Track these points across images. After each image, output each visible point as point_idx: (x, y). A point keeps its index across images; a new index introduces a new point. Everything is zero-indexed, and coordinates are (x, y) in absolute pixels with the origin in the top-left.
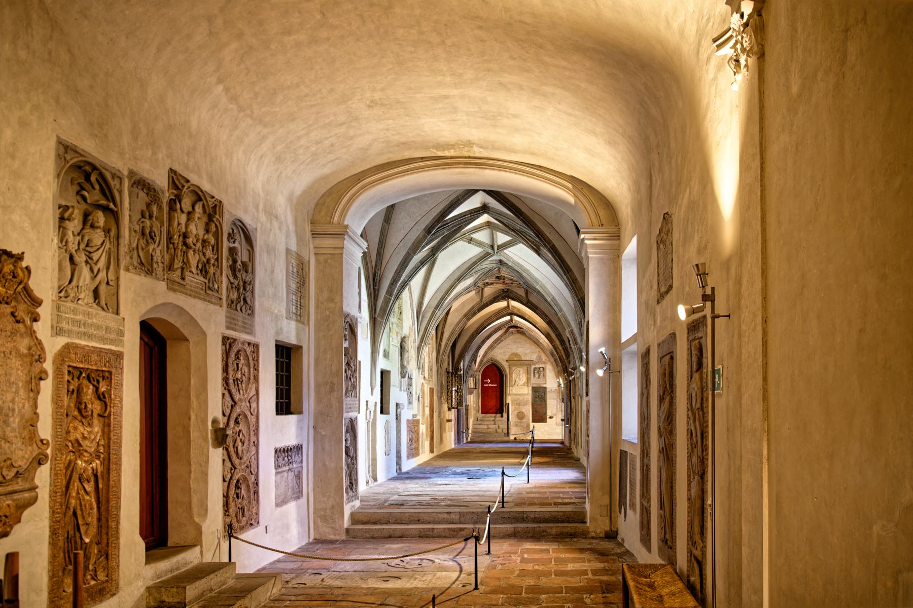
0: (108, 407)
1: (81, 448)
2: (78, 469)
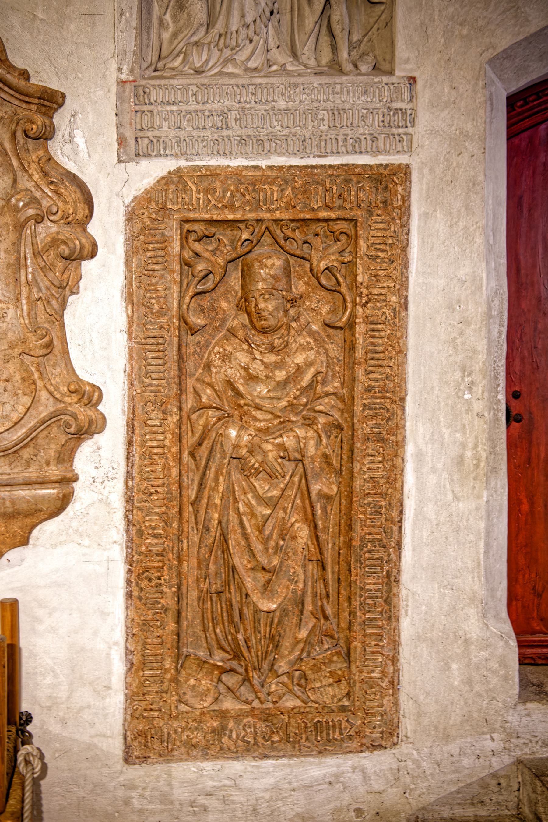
0: (349, 305)
1: (242, 402)
2: (228, 449)
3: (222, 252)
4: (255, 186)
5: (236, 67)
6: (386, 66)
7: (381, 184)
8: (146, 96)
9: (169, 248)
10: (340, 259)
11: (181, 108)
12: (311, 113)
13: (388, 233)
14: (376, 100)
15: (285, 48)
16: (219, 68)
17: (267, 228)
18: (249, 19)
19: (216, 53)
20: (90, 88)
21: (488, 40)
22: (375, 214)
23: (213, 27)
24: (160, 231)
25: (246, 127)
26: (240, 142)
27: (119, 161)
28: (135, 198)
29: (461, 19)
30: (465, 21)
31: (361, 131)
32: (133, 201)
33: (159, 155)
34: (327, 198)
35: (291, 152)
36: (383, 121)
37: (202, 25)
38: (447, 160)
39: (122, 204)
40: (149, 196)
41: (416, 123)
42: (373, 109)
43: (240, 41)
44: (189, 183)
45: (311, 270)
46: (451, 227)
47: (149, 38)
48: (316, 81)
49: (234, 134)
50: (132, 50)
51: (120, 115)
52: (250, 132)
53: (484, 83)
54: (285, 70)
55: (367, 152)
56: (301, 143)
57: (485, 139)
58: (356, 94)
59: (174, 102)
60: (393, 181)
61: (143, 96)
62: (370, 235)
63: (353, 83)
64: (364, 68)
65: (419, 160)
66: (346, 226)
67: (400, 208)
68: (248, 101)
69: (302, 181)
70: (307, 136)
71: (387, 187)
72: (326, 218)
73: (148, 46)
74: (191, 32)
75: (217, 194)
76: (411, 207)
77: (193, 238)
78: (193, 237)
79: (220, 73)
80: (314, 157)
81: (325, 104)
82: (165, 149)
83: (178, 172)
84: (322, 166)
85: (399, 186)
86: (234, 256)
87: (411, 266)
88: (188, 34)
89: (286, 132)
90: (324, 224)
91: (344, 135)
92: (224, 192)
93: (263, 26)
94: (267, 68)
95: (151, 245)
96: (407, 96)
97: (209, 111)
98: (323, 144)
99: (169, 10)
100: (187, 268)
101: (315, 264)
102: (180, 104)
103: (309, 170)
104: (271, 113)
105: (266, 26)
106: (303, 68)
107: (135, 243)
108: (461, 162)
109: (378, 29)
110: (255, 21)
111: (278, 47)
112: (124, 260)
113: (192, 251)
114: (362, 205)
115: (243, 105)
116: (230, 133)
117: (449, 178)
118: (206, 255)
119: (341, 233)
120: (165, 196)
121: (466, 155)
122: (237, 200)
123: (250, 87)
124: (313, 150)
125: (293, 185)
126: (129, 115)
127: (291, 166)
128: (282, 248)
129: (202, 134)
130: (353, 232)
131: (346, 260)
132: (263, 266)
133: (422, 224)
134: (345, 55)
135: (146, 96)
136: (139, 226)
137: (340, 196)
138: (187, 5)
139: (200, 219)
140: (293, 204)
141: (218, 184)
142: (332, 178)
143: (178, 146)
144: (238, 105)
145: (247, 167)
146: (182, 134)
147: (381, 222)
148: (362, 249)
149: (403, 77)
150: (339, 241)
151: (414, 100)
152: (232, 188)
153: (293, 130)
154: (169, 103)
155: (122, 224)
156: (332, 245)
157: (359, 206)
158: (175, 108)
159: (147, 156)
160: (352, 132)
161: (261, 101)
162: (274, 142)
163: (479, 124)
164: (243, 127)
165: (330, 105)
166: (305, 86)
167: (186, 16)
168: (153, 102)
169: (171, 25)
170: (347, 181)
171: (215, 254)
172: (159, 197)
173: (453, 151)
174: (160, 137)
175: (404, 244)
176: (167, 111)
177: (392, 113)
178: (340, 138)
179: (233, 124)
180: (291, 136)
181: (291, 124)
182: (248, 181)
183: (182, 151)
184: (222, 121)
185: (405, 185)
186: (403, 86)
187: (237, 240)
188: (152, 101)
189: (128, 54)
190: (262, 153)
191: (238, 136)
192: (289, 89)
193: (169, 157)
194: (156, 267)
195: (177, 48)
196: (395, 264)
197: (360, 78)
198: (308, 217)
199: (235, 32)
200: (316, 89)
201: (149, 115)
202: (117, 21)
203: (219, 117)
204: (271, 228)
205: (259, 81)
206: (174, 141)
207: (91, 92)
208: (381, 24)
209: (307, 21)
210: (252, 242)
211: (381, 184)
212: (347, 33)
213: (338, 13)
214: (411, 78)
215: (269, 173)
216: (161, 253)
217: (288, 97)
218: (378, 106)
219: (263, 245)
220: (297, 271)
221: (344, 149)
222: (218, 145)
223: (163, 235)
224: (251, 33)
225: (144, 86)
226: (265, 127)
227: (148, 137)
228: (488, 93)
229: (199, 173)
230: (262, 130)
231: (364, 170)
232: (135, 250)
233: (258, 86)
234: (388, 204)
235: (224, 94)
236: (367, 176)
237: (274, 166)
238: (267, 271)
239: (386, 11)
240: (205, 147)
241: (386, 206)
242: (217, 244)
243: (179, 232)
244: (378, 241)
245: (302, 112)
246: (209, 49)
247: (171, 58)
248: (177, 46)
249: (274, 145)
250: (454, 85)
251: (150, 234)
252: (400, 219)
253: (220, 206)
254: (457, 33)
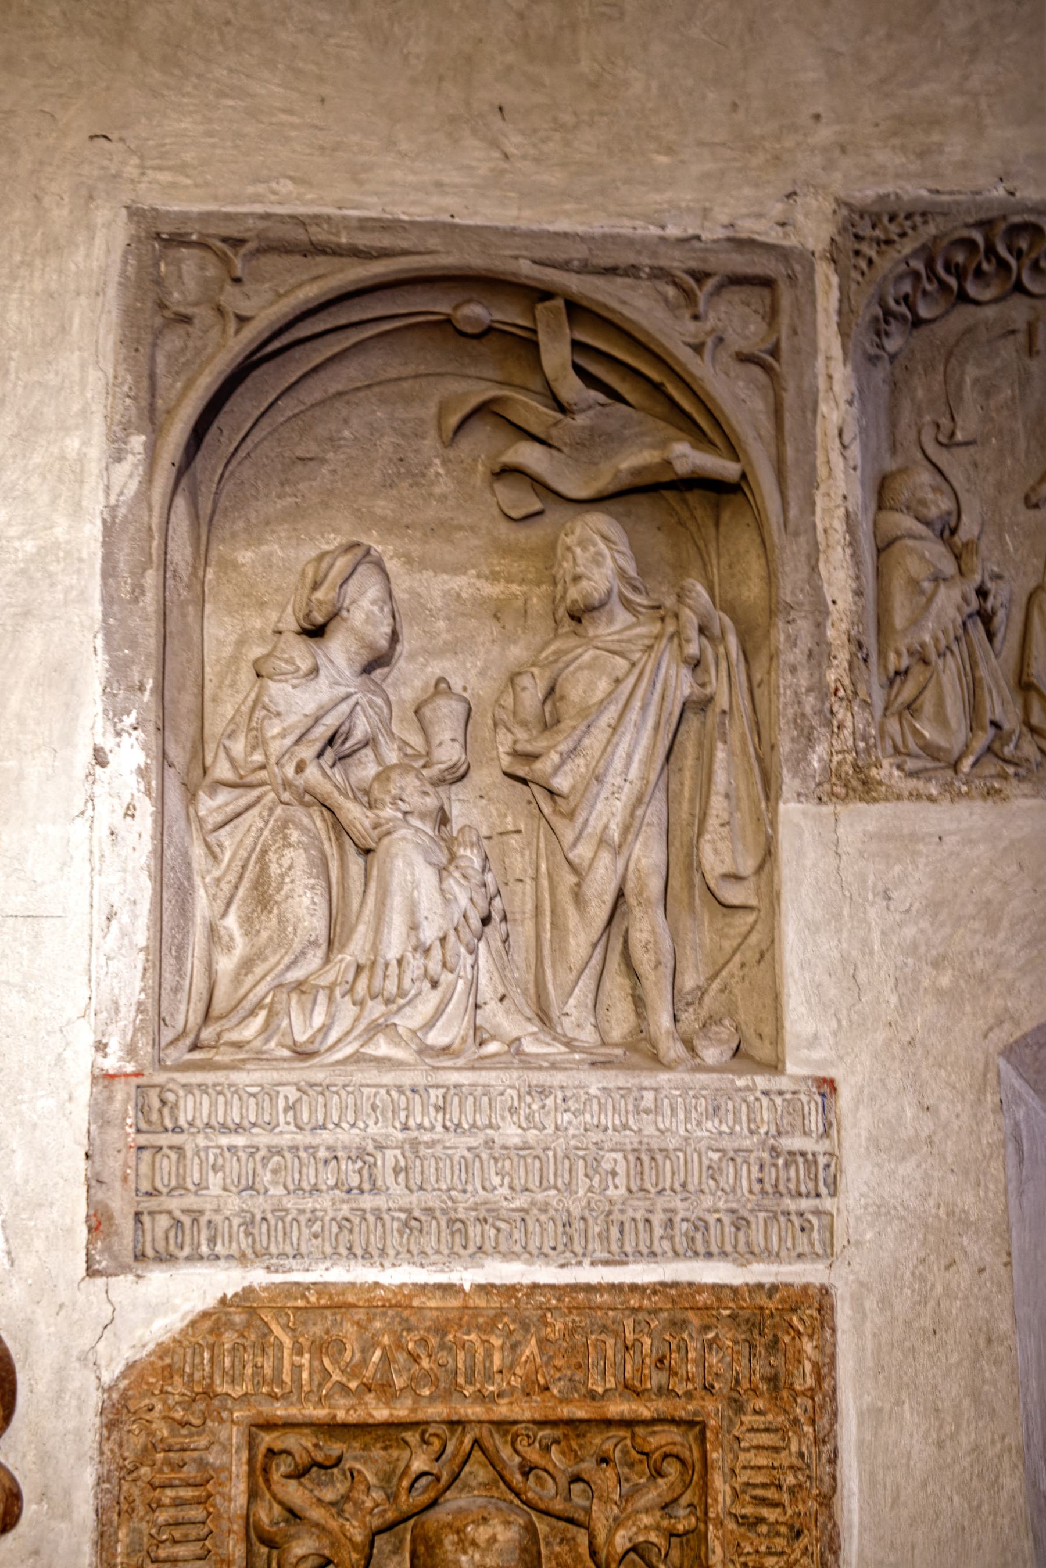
3: (358, 1505)
4: (445, 1334)
5: (397, 1045)
6: (763, 1051)
7: (761, 1334)
8: (166, 1111)
9: (218, 1500)
10: (665, 1523)
11: (256, 1140)
12: (583, 1158)
13: (784, 1459)
14: (742, 1128)
15: (520, 999)
16: (355, 1046)
17: (476, 1442)
18: (429, 934)
19: (347, 1011)
20: (22, 1091)
21: (1000, 1002)
22: (749, 1408)
23: (343, 946)
24: (196, 1454)
25: (421, 1188)
26: (406, 1224)
27: (91, 1272)
28: (130, 1367)
29: (934, 952)
30: (944, 958)
31: (708, 1202)
32: (123, 1375)
33: (196, 1257)
34: (628, 1367)
35: (535, 1252)
36: (761, 1181)
37: (314, 944)
38: (922, 1279)
39: (94, 1383)
40: (168, 1361)
41: (841, 1187)
42: (736, 1151)
43: (407, 983)
44: (274, 1326)
45: (593, 1553)
46: (940, 1445)
47: (180, 971)
48: (595, 1082)
49: (391, 1205)
50: (134, 1000)
51: (97, 1158)
52: (432, 1200)
53: (997, 1099)
54: (519, 1052)
55: (724, 1254)
56: (560, 1229)
57: (1009, 1230)
58: (694, 1115)
59: (239, 1126)
60: (791, 1326)
61: (160, 1111)
62: (739, 1464)
63: (685, 1090)
64: (711, 1054)
65: (851, 1277)
66: (678, 1439)
67: (810, 1394)
68: (427, 1124)
69: (565, 1324)
70: (576, 1213)
71: (776, 1340)
72: (627, 1416)
73: (176, 990)
74: (287, 960)
75: (347, 1355)
76: (839, 1392)
77: (283, 1469)
78: (282, 1467)
79: (357, 1059)
80: (593, 1264)
81: (617, 1137)
82: (212, 1241)
83: (247, 1299)
84: (612, 1286)
85: (805, 1339)
86: (390, 1516)
87: (845, 1546)
88: (278, 963)
89: (521, 1201)
90: (622, 1433)
91: (665, 1211)
92: (366, 1351)
93: (463, 950)
94: (474, 1049)
95: (170, 1493)
96: (815, 1122)
97: (328, 1148)
98: (614, 1232)
99: (233, 908)
100: (264, 1550)
101: (601, 1538)
102: (255, 1130)
103: (581, 1296)
104: (485, 1156)
105: (473, 951)
106: (563, 1049)
107: (125, 1486)
108: (954, 1285)
109: (743, 965)
110: (443, 940)
111: (502, 999)
112: (95, 1536)
113: (281, 1503)
114: (717, 1386)
115: (415, 1134)
116: (381, 1201)
117: (926, 1322)
118: (316, 1514)
119: (666, 1456)
120: (212, 1360)
121: (965, 1272)
122: (399, 1372)
123: (433, 1092)
124: (590, 1247)
125: (543, 1334)
126: (121, 1156)
127: (535, 1286)
128: (518, 1495)
129: (309, 1204)
130: (696, 1455)
131: (680, 1528)
132: (465, 1543)
133: (868, 1437)
134: (665, 1021)
135: (166, 1111)
136: (138, 1441)
137: (661, 1360)
138: (278, 898)
139: (300, 1419)
140: (542, 1381)
141: (349, 1329)
142: (640, 1316)
143: (248, 1234)
144: (400, 1136)
145: (424, 1286)
146: (259, 1205)
147: (767, 1430)
148: (720, 1498)
149: (805, 1078)
150: (661, 1475)
151: (834, 1132)
152: (386, 1340)
153: (540, 1197)
154: (225, 1128)
155: (91, 1439)
156: (644, 1486)
157: (709, 1389)
158: (240, 1140)
159: (166, 1258)
160: (686, 1204)
161: (458, 1125)
162: (494, 1226)
163: (991, 1195)
164: (414, 1187)
165: (629, 1139)
166: (569, 1094)
167: (274, 921)
168: (185, 1126)
169: (239, 940)
170: (678, 1325)
171: (341, 1513)
172: (193, 1365)
173: (932, 1258)
174: (201, 1212)
175: (826, 1489)
176: (220, 1147)
177: (781, 1162)
178: (657, 1219)
179: (390, 1180)
180: (535, 1211)
181: (534, 1183)
182: (428, 1324)
183: (258, 1247)
184: (360, 1171)
185: (822, 1337)
186: (804, 1099)
187: (399, 1472)
188: (182, 1122)
189: (123, 1010)
190: (462, 1252)
191: (401, 1210)
192: (528, 1099)
193: (222, 1263)
194: (182, 1551)
195: (251, 996)
196: (804, 1541)
197: (702, 1077)
198: (581, 1414)
199: (394, 963)
200: (595, 1101)
201: (174, 1156)
202: (97, 934)
203: (354, 1162)
204: (487, 1443)
205: (454, 1077)
206: (236, 1222)
207: (23, 1102)
208: (751, 956)
209: (572, 942)
210: (438, 1479)
211: (761, 1334)
212: (669, 972)
213: (645, 925)
214: (824, 1080)
215: (481, 1302)
216: (196, 1513)
217: (527, 1118)
218: (747, 1143)
219: (466, 1487)
220: (557, 1556)
221: (666, 1245)
222: (351, 1231)
223: (202, 1464)
224: (434, 965)
225: (162, 1088)
226: (470, 1188)
227: (169, 1213)
228: (1007, 1123)
229: (300, 1303)
230: (460, 1197)
231: (719, 1299)
232: (125, 1506)
233: (452, 1091)
234: (782, 1384)
235: (367, 1107)
236: (727, 1312)
237: (493, 1286)
238: (477, 1557)
239: (759, 927)
240: (316, 1236)
241: (776, 1388)
242: (348, 1483)
243: (245, 1456)
244: (760, 1479)
245: (560, 1154)
246: (331, 999)
247: (234, 1019)
248: (250, 991)
249: (493, 1232)
250: (926, 1102)
251: (167, 1462)
252: (813, 1422)
253: (353, 1385)
254: (926, 983)
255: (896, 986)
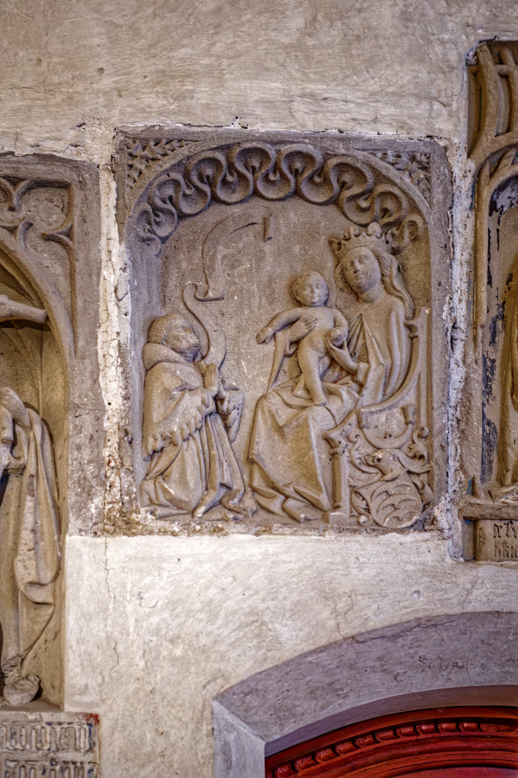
42: (26, 761)
53: (210, 728)
96: (83, 742)
151: (96, 749)
177: (58, 768)
186: (77, 727)
214: (91, 715)
218: (34, 756)
250: (161, 730)
255: (144, 654)
